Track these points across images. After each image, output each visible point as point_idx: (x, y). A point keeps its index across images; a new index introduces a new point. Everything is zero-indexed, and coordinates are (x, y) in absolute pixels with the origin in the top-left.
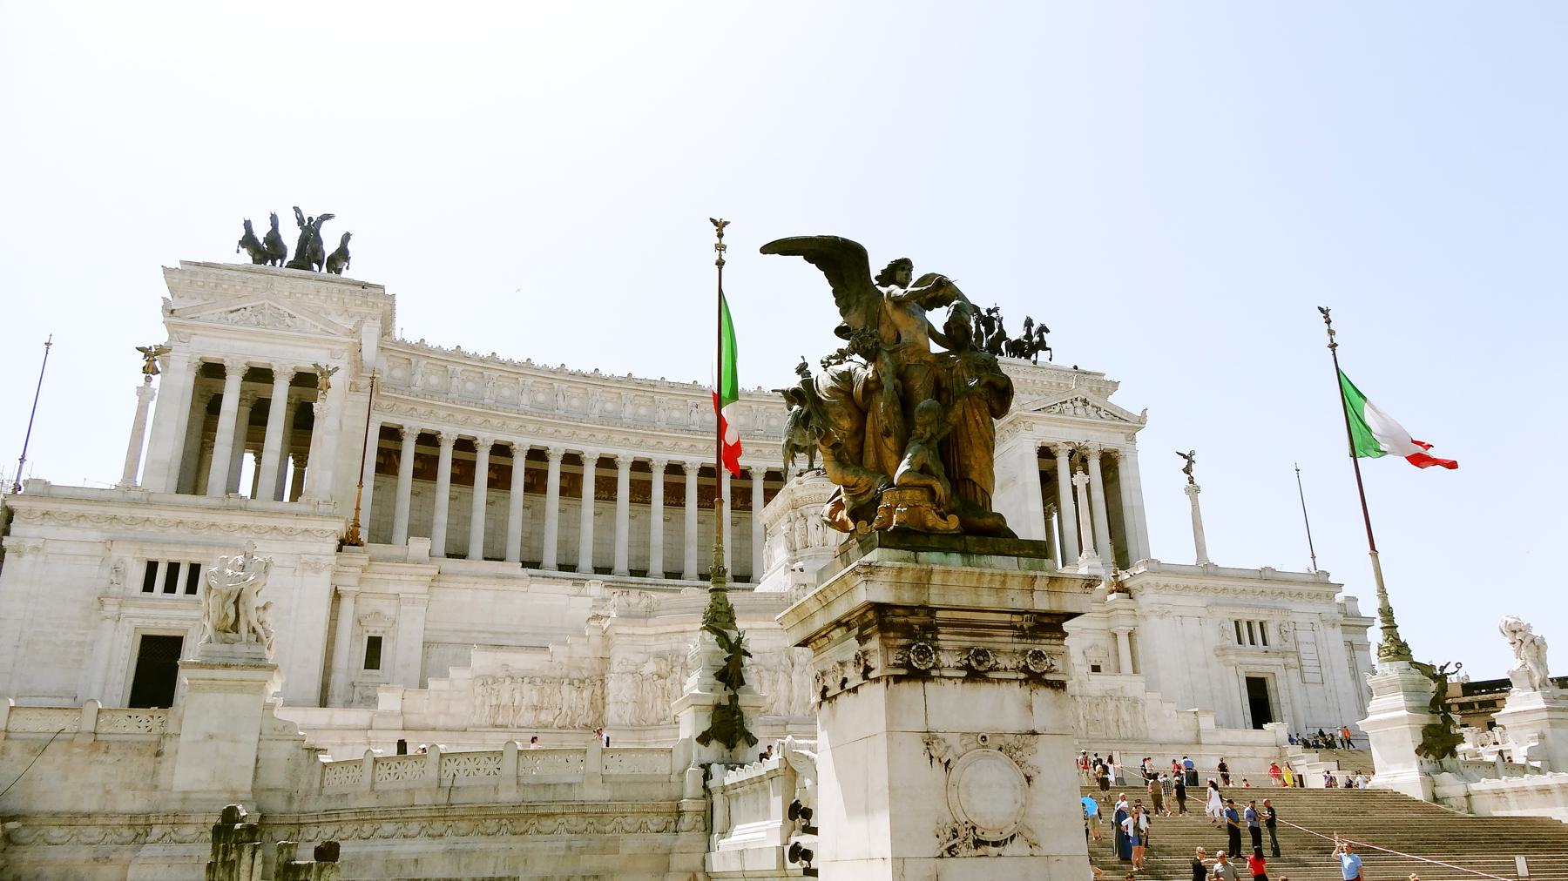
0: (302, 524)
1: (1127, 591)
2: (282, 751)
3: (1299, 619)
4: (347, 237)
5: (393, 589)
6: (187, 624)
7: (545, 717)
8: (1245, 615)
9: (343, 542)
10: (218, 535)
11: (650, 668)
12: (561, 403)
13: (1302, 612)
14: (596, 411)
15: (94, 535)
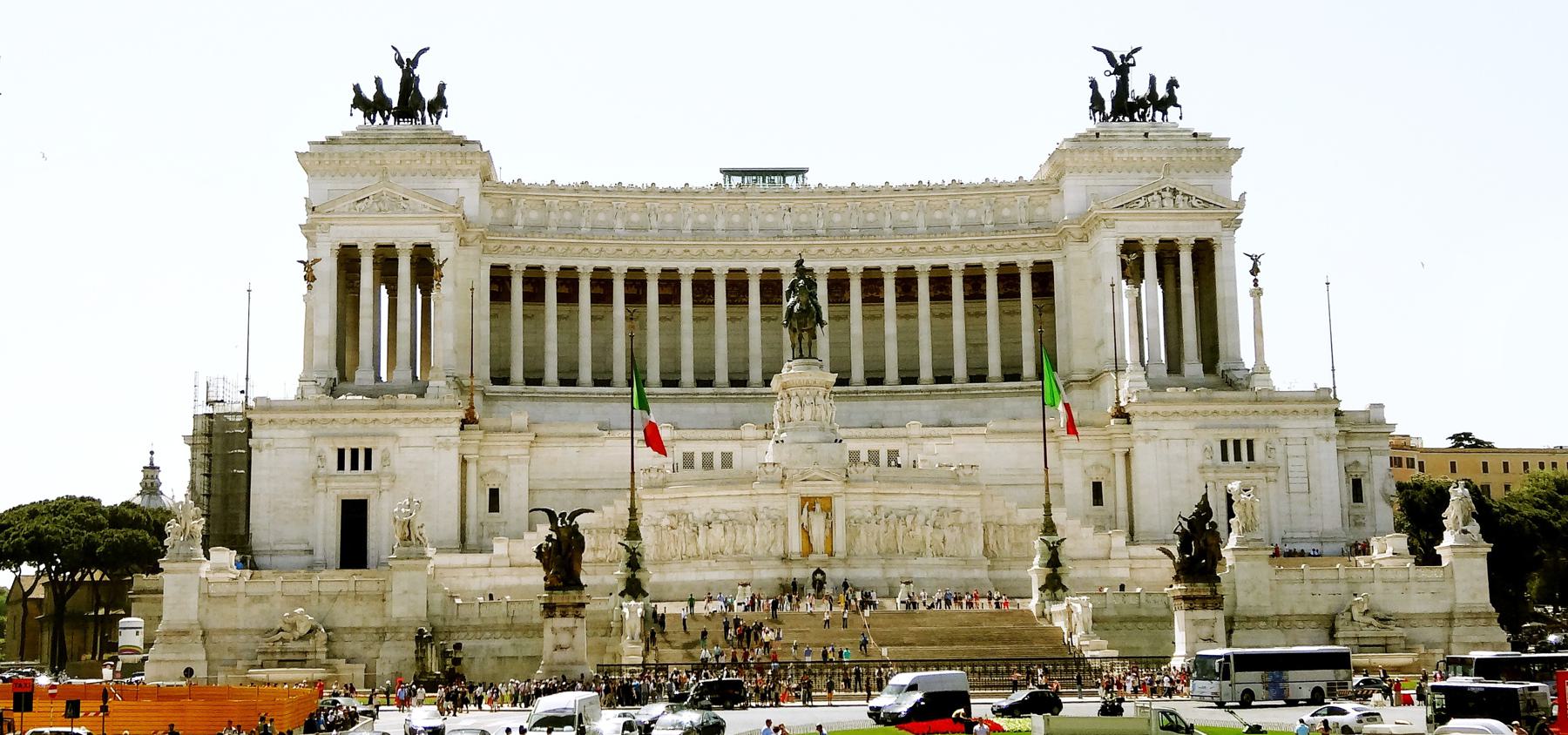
0: (434, 415)
1: (1127, 416)
2: (438, 598)
3: (1290, 434)
4: (442, 87)
5: (503, 453)
6: (369, 492)
7: (600, 555)
8: (1231, 436)
9: (464, 422)
10: (380, 428)
11: (666, 522)
12: (654, 223)
13: (1295, 427)
14: (689, 226)
15: (302, 433)
